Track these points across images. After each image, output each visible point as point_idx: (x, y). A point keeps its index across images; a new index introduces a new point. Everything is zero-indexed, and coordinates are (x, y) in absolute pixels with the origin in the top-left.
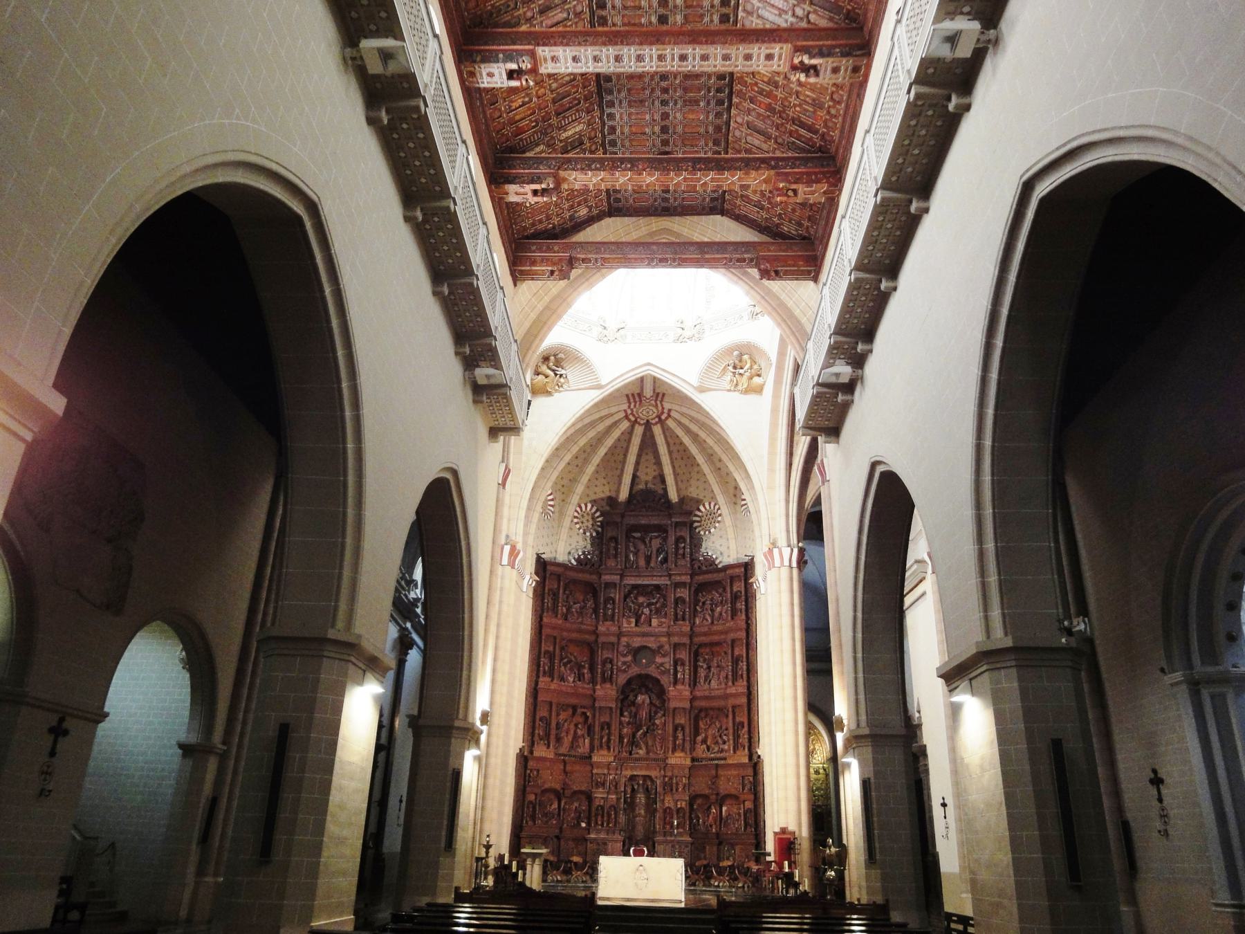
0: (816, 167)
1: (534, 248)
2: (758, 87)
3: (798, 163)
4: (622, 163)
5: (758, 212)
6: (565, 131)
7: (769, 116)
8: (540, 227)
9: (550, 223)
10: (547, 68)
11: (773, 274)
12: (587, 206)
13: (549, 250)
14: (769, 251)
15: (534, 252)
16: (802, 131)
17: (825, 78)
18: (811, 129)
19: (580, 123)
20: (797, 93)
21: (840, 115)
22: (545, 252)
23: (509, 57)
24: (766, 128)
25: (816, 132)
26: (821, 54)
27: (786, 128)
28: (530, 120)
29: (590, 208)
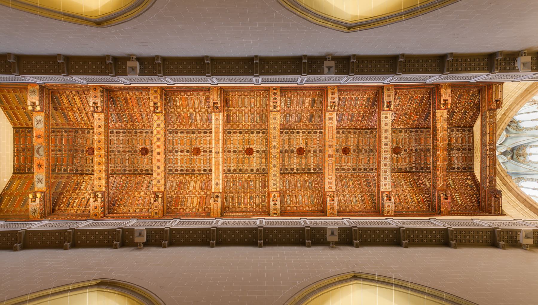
0: (435, 95)
1: (483, 204)
2: (408, 119)
3: (434, 102)
4: (434, 166)
5: (468, 113)
6: (426, 185)
7: (419, 114)
8: (474, 200)
9: (473, 196)
10: (389, 188)
11: (498, 103)
12: (466, 180)
13: (484, 198)
14: (485, 106)
15: (485, 204)
16: (424, 102)
17: (392, 99)
18: (422, 99)
19: (423, 180)
20: (407, 106)
21: (413, 91)
22: (485, 199)
23: (383, 200)
24: (425, 115)
25: (423, 97)
26: (384, 102)
27: (423, 108)
28: (418, 196)
29: (467, 179)
